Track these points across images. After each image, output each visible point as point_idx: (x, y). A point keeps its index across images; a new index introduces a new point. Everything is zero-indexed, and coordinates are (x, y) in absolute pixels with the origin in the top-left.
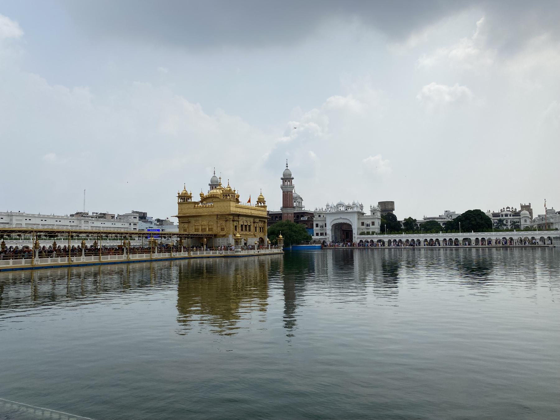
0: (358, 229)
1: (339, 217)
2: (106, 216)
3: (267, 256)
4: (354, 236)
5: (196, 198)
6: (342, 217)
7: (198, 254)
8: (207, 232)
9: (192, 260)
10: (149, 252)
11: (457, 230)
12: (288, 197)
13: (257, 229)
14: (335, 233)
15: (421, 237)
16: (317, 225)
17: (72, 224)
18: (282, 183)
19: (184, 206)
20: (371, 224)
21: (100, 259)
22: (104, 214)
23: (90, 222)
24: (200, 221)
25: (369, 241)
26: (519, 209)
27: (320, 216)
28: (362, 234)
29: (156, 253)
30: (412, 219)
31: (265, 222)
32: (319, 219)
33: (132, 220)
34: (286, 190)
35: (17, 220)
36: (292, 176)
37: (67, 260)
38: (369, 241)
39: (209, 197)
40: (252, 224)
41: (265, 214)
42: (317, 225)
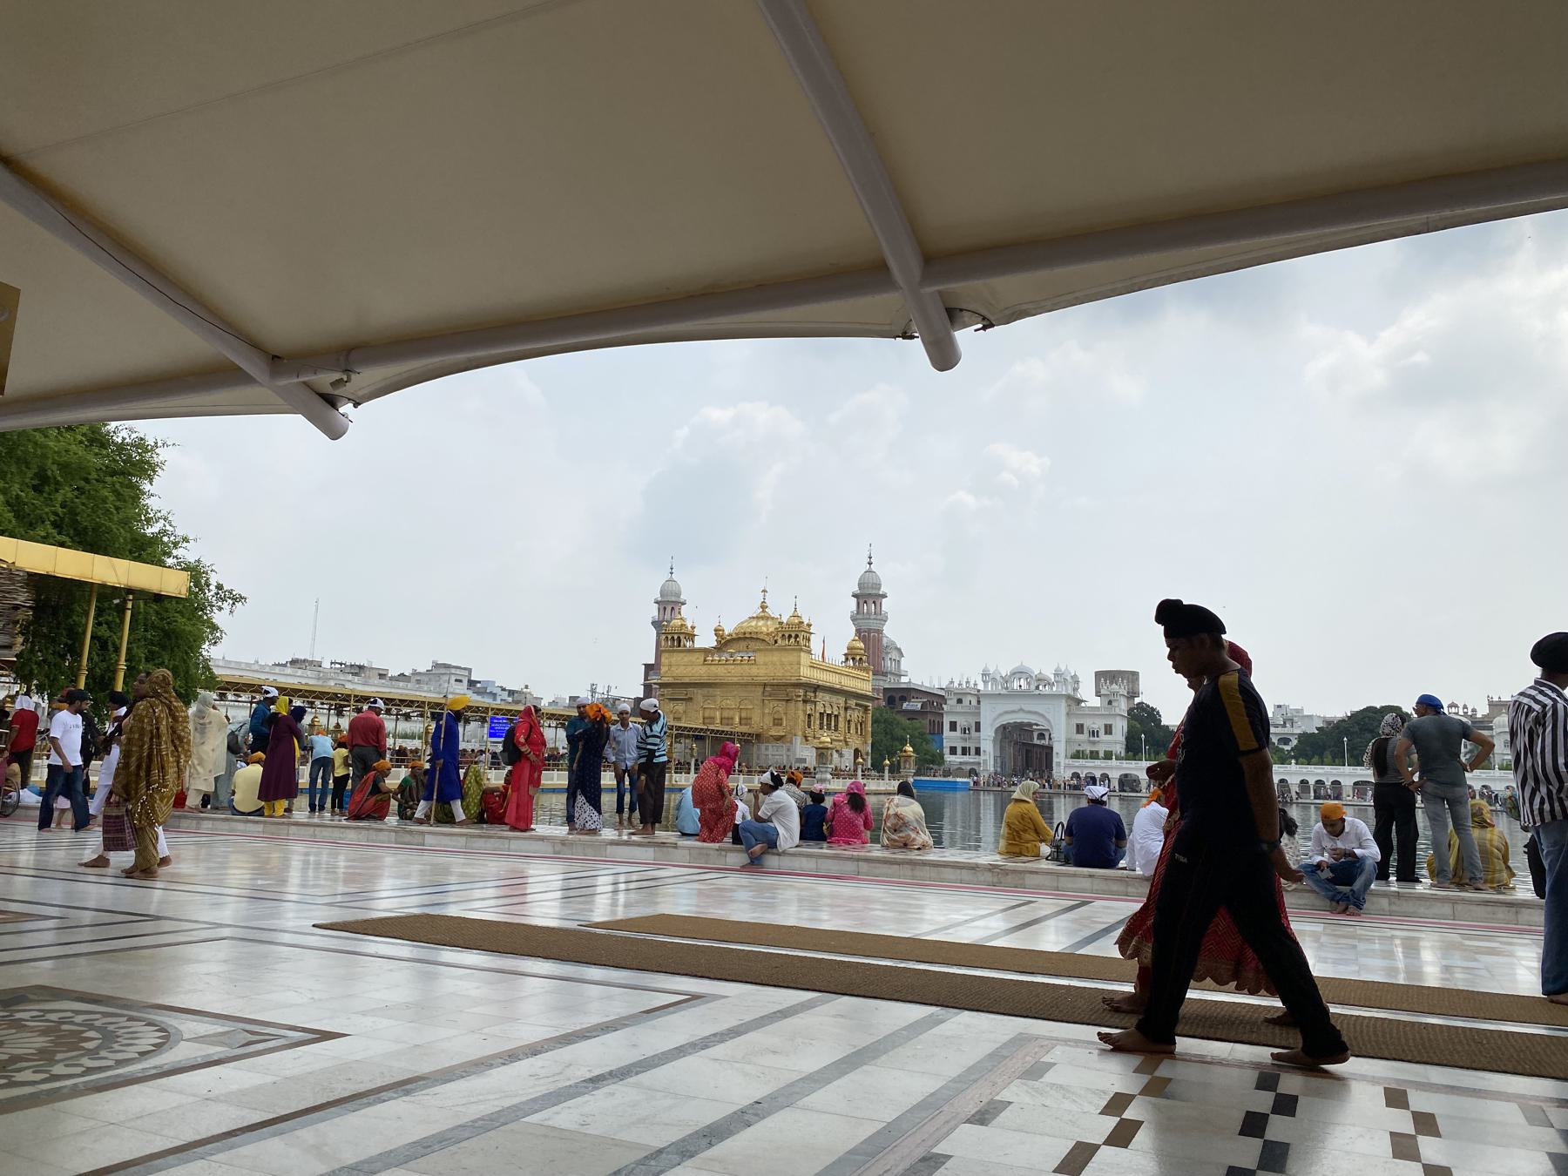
0: (1068, 741)
1: (1015, 707)
6: (1026, 708)
11: (1338, 759)
12: (870, 647)
14: (1002, 748)
16: (953, 726)
18: (854, 608)
20: (1102, 732)
22: (361, 667)
24: (719, 699)
26: (1483, 711)
27: (960, 701)
28: (1077, 755)
31: (866, 708)
32: (959, 708)
34: (865, 625)
42: (953, 726)
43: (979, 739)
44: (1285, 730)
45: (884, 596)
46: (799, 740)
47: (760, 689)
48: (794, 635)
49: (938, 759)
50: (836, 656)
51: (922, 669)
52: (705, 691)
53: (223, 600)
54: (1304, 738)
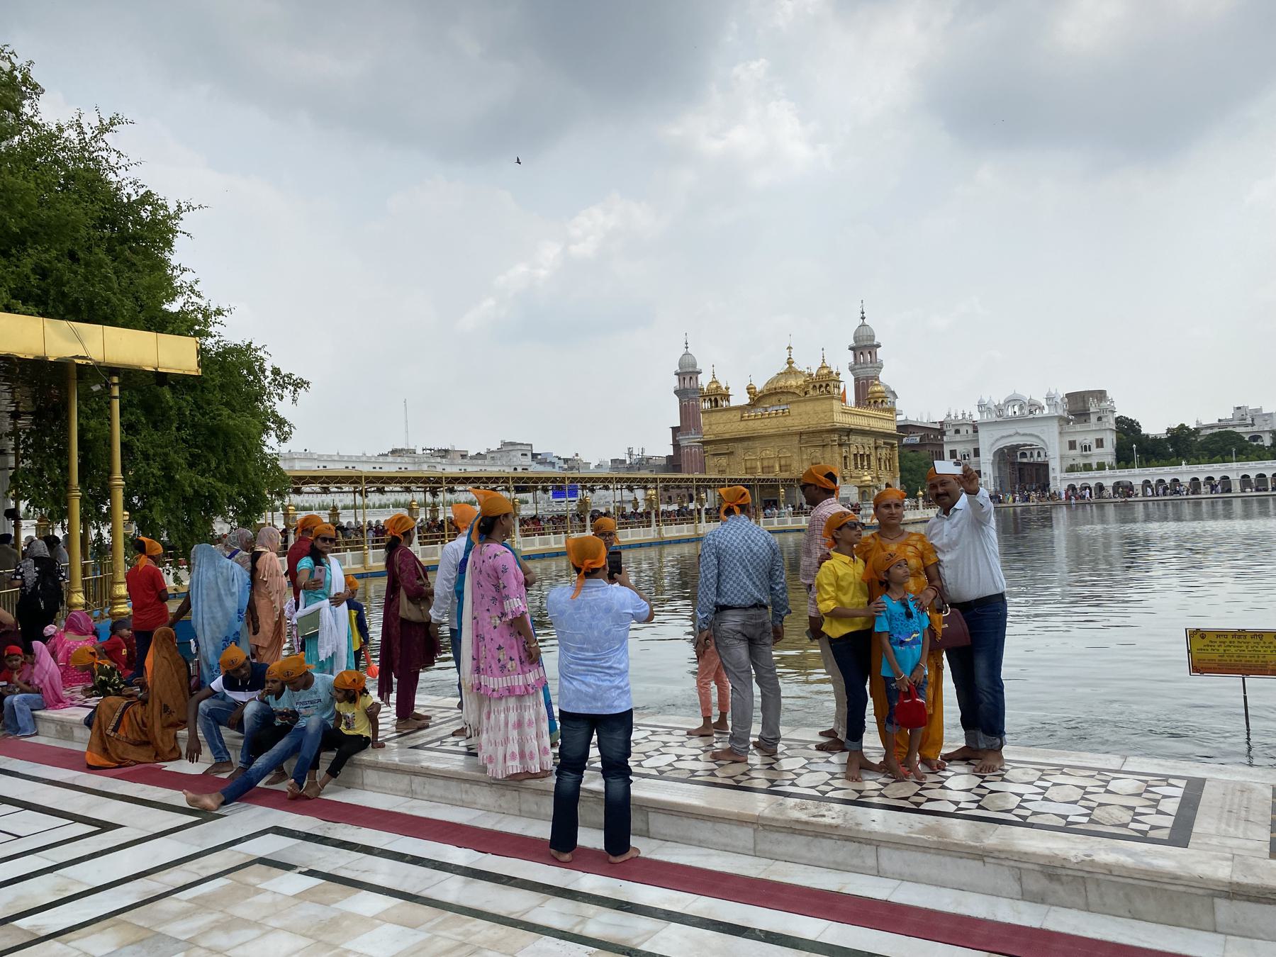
0: (1062, 457)
1: (1012, 432)
4: (1051, 475)
12: (869, 394)
14: (999, 468)
15: (1231, 470)
20: (1094, 446)
22: (446, 451)
24: (758, 450)
25: (1092, 484)
28: (1072, 469)
29: (704, 523)
30: (1187, 428)
31: (892, 445)
32: (958, 438)
34: (862, 373)
37: (563, 541)
38: (1092, 484)
40: (873, 451)
41: (891, 428)
43: (978, 463)
44: (1255, 428)
47: (797, 438)
51: (919, 402)
53: (283, 387)
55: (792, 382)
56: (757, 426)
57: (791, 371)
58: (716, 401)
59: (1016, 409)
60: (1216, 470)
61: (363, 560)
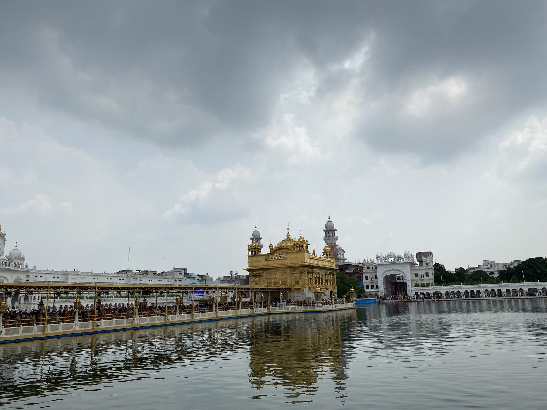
0: (412, 280)
1: (391, 269)
2: (149, 273)
3: (343, 311)
4: (408, 288)
5: (266, 250)
6: (394, 269)
7: (277, 310)
8: (281, 286)
9: (271, 317)
10: (234, 309)
12: (332, 250)
13: (329, 282)
15: (481, 288)
17: (122, 282)
18: (325, 235)
19: (255, 259)
21: (192, 317)
22: (147, 271)
23: (139, 279)
24: (272, 274)
27: (368, 268)
28: (416, 285)
29: (241, 310)
31: (333, 274)
32: (368, 271)
33: (177, 276)
34: (329, 241)
35: (72, 279)
36: (335, 228)
39: (279, 249)
40: (324, 276)
41: (332, 264)
42: (367, 278)
44: (492, 270)
45: (336, 230)
46: (306, 290)
48: (301, 246)
49: (363, 291)
50: (319, 253)
51: (353, 255)
52: (267, 271)
54: (501, 272)
55: (289, 244)
56: (273, 263)
57: (288, 239)
58: (255, 251)
59: (392, 259)
60: (475, 287)
61: (44, 330)
